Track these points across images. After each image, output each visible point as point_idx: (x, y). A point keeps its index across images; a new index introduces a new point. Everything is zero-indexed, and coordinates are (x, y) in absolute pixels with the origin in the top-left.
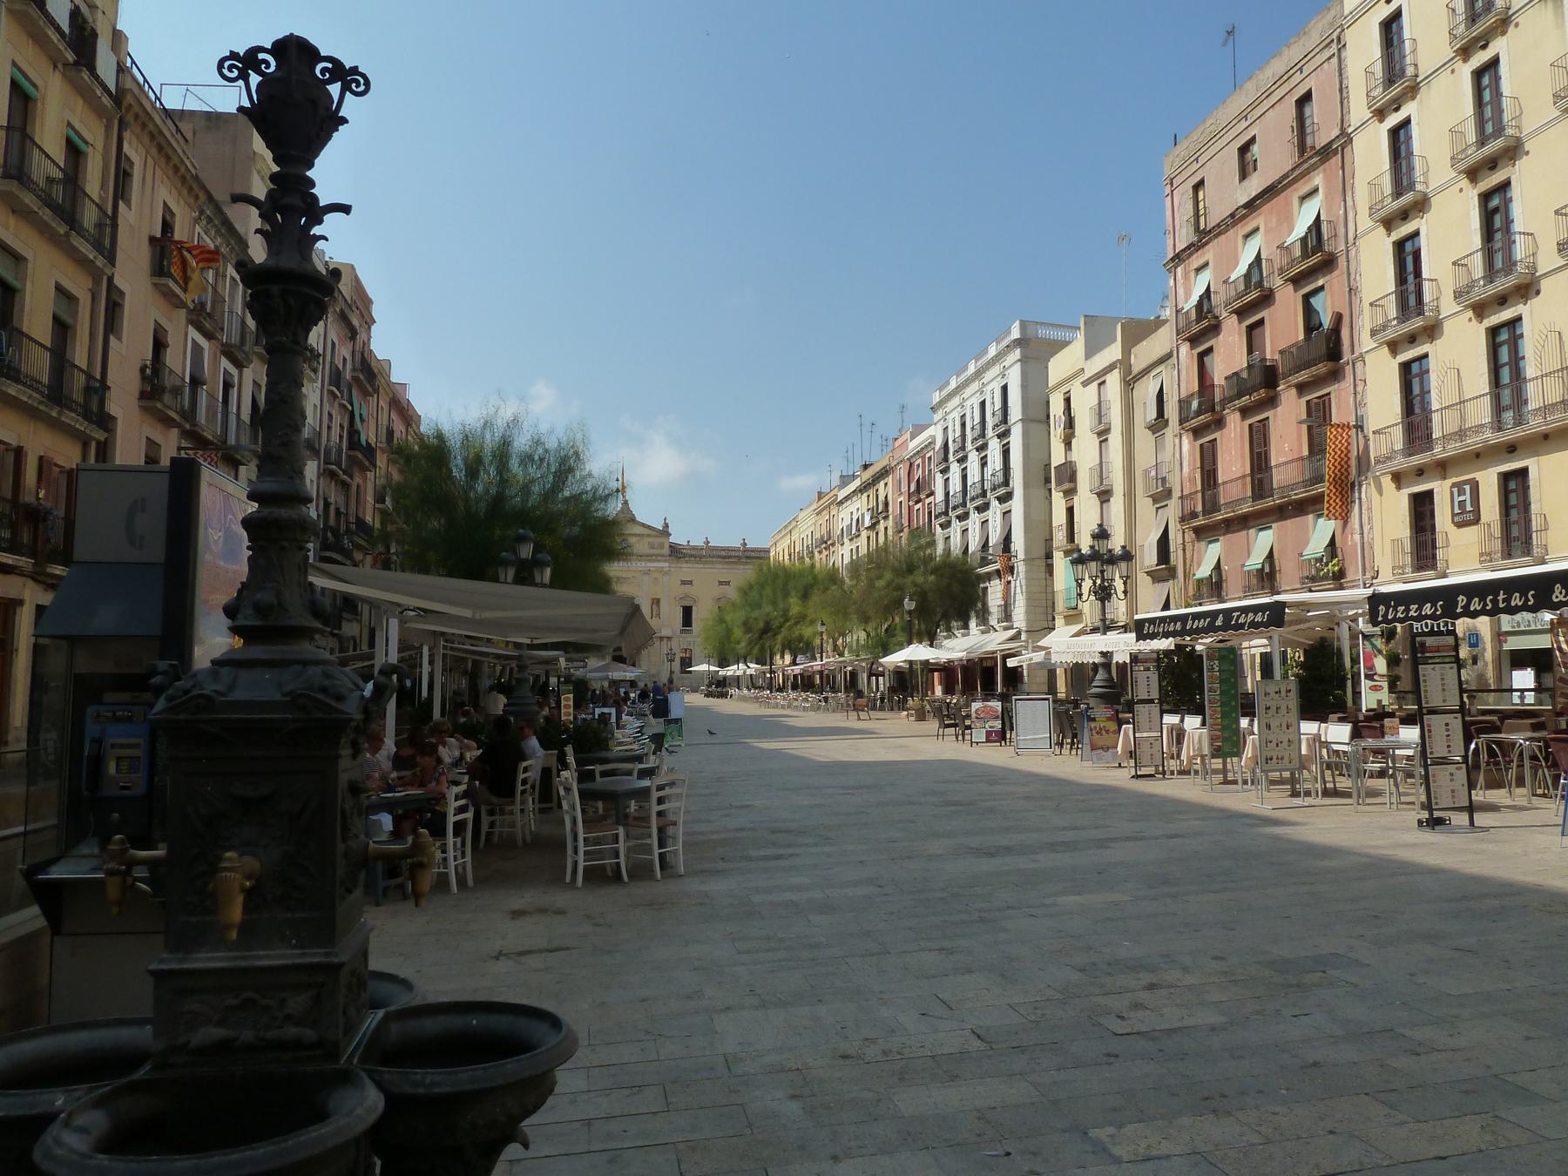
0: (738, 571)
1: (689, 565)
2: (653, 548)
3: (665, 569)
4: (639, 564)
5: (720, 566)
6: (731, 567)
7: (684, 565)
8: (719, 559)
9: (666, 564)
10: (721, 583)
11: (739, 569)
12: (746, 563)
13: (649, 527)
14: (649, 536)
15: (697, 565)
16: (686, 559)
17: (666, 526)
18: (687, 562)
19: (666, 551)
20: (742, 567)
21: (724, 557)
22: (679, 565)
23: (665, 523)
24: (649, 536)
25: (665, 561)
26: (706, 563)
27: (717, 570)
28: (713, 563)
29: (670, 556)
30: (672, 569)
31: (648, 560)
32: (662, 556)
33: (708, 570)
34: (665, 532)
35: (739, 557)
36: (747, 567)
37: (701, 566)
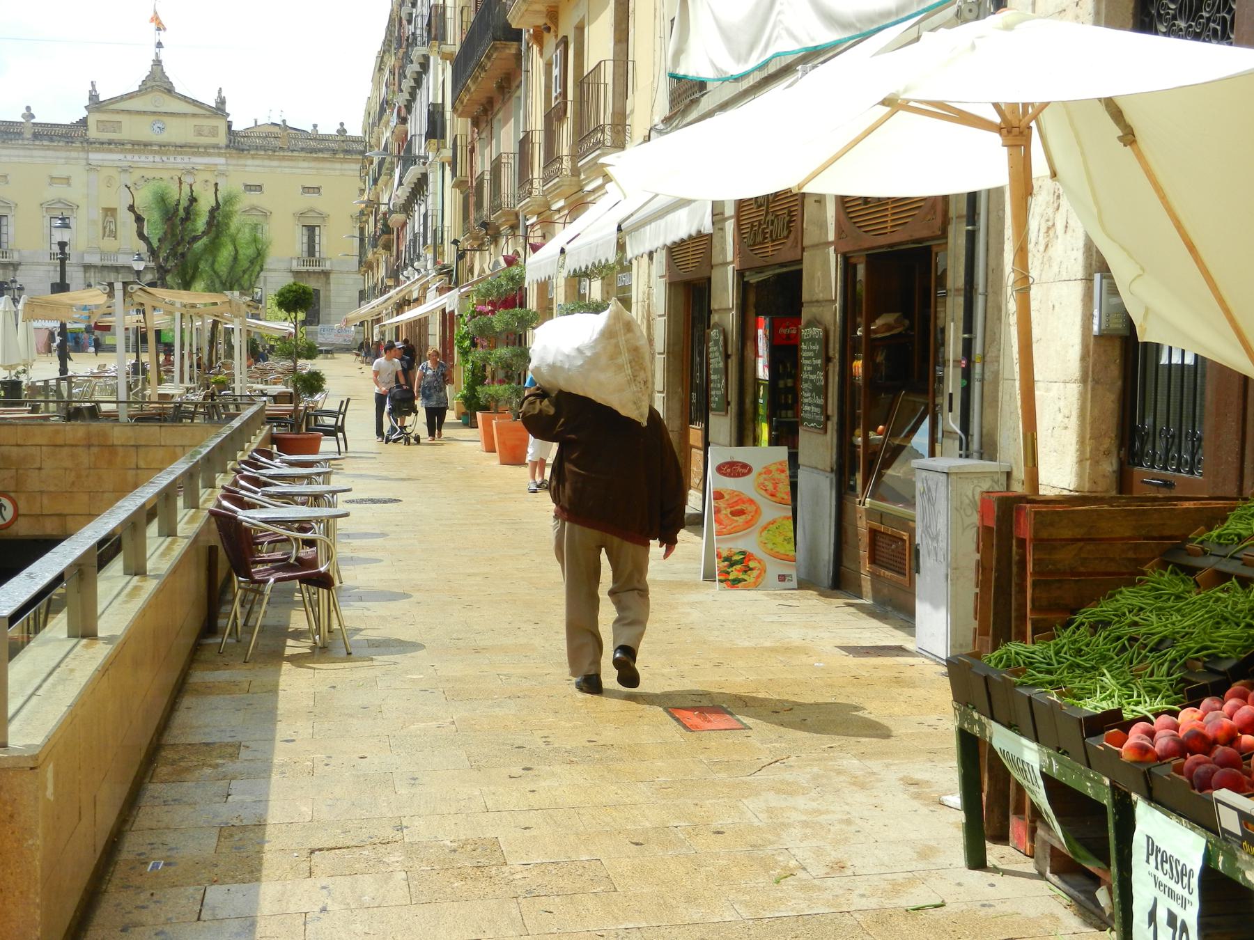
0: (332, 173)
1: (257, 162)
2: (201, 135)
3: (220, 168)
4: (179, 159)
5: (305, 164)
6: (321, 165)
7: (250, 162)
8: (303, 154)
9: (222, 160)
10: (306, 189)
11: (334, 169)
12: (344, 160)
13: (195, 102)
14: (194, 115)
15: (267, 163)
16: (252, 152)
17: (222, 102)
18: (253, 157)
19: (222, 139)
20: (338, 166)
21: (313, 151)
22: (242, 162)
23: (220, 96)
24: (194, 115)
25: (219, 155)
26: (283, 158)
27: (300, 171)
28: (291, 159)
29: (228, 147)
30: (231, 168)
31: (193, 154)
32: (216, 147)
33: (287, 170)
34: (220, 109)
35: (335, 152)
36: (346, 166)
37: (275, 163)
